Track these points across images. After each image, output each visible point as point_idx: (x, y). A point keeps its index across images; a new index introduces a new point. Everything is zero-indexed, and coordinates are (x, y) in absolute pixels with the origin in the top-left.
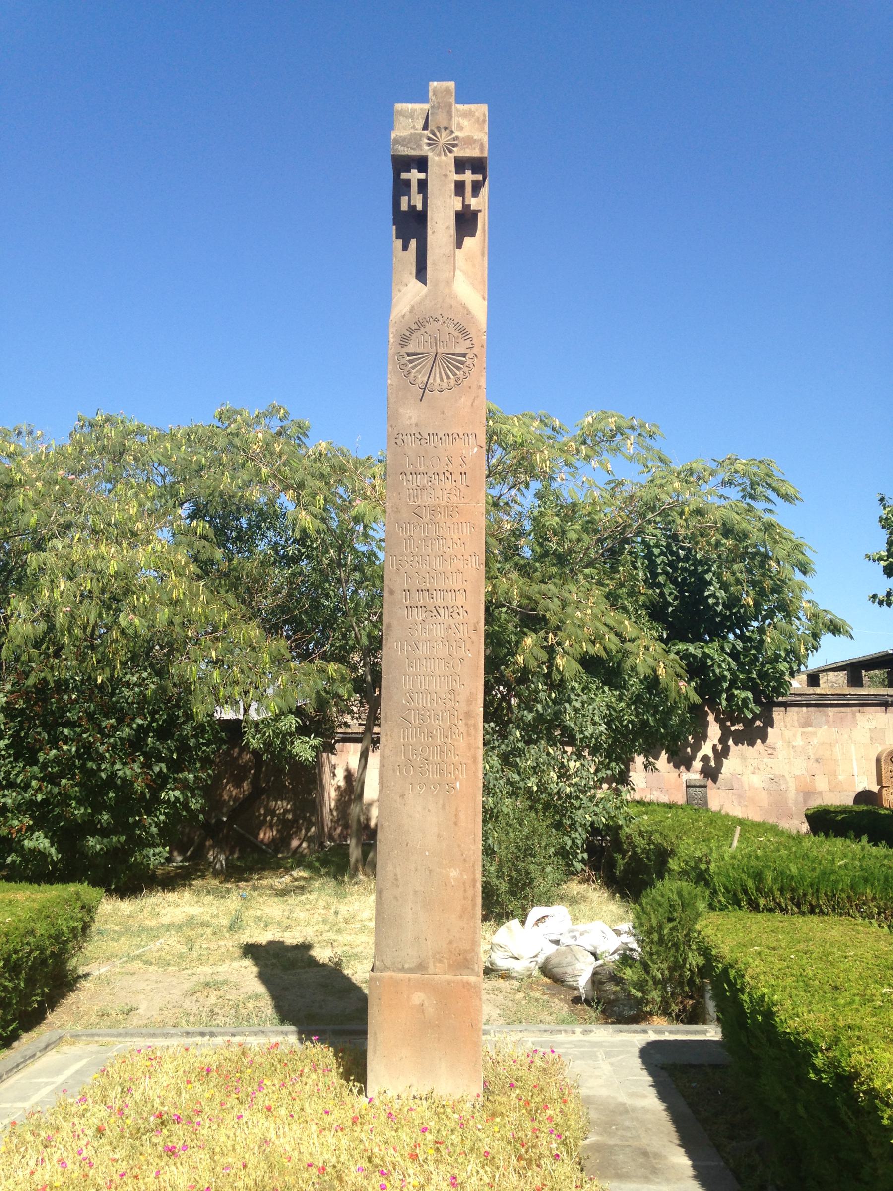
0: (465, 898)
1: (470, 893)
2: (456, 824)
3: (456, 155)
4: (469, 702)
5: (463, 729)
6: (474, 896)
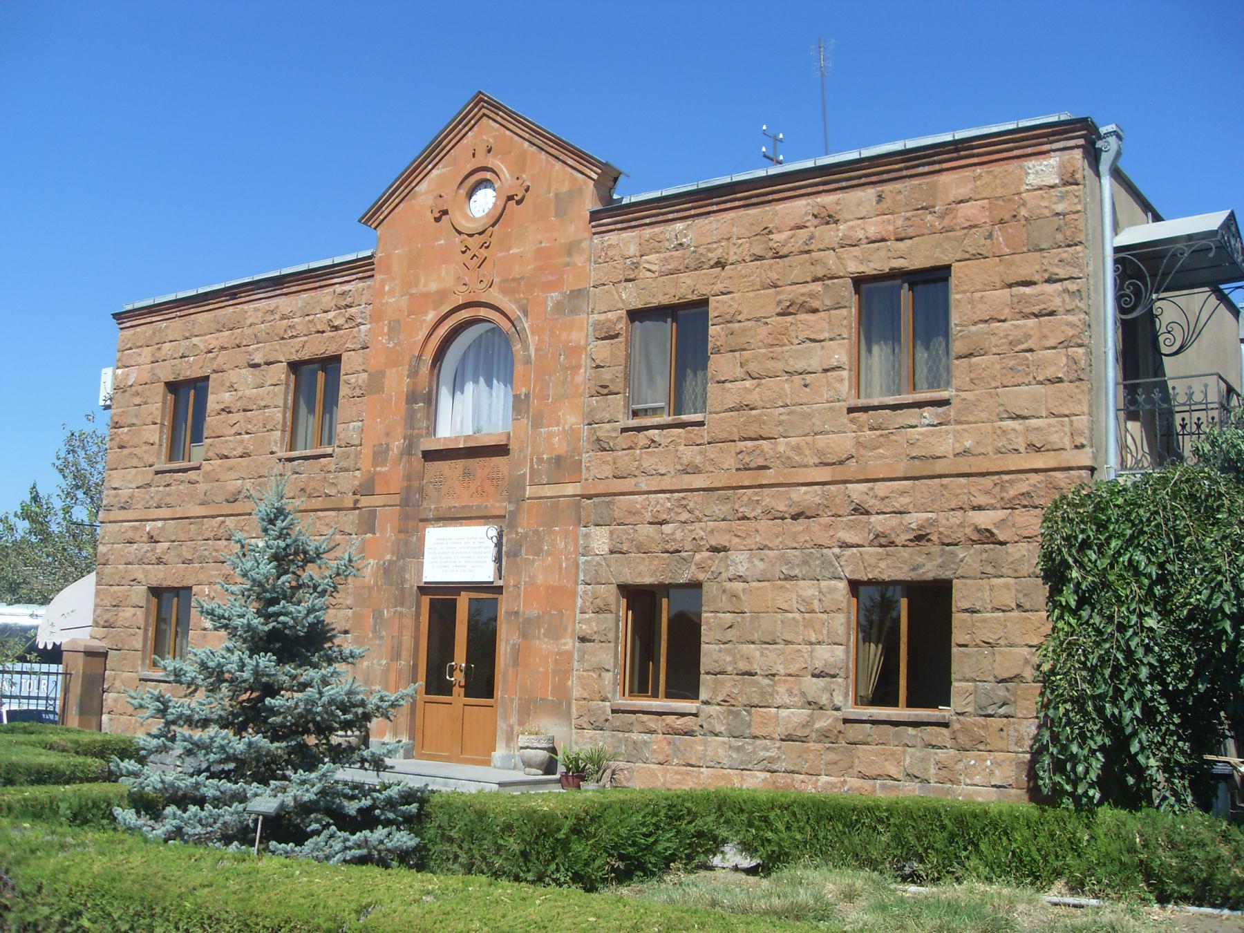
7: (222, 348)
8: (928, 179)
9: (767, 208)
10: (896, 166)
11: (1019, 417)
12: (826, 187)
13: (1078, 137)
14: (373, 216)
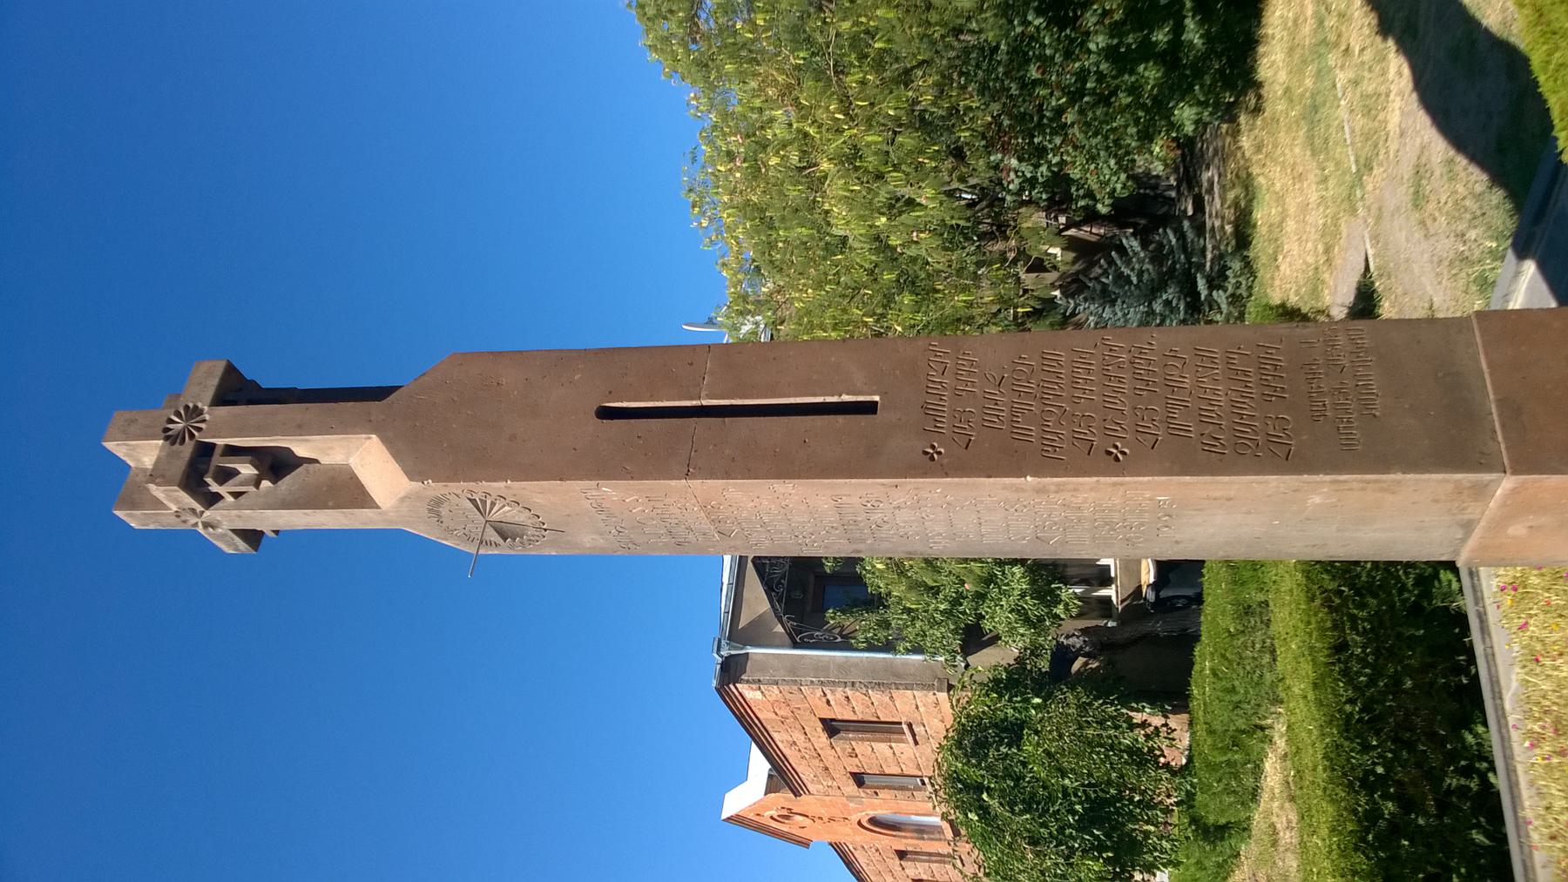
0: (1363, 489)
1: (1355, 485)
2: (1230, 499)
3: (203, 509)
4: (1018, 490)
5: (1067, 495)
6: (1361, 481)
7: (893, 875)
8: (763, 722)
9: (788, 757)
10: (757, 730)
11: (917, 707)
12: (773, 744)
13: (730, 689)
14: (805, 843)
